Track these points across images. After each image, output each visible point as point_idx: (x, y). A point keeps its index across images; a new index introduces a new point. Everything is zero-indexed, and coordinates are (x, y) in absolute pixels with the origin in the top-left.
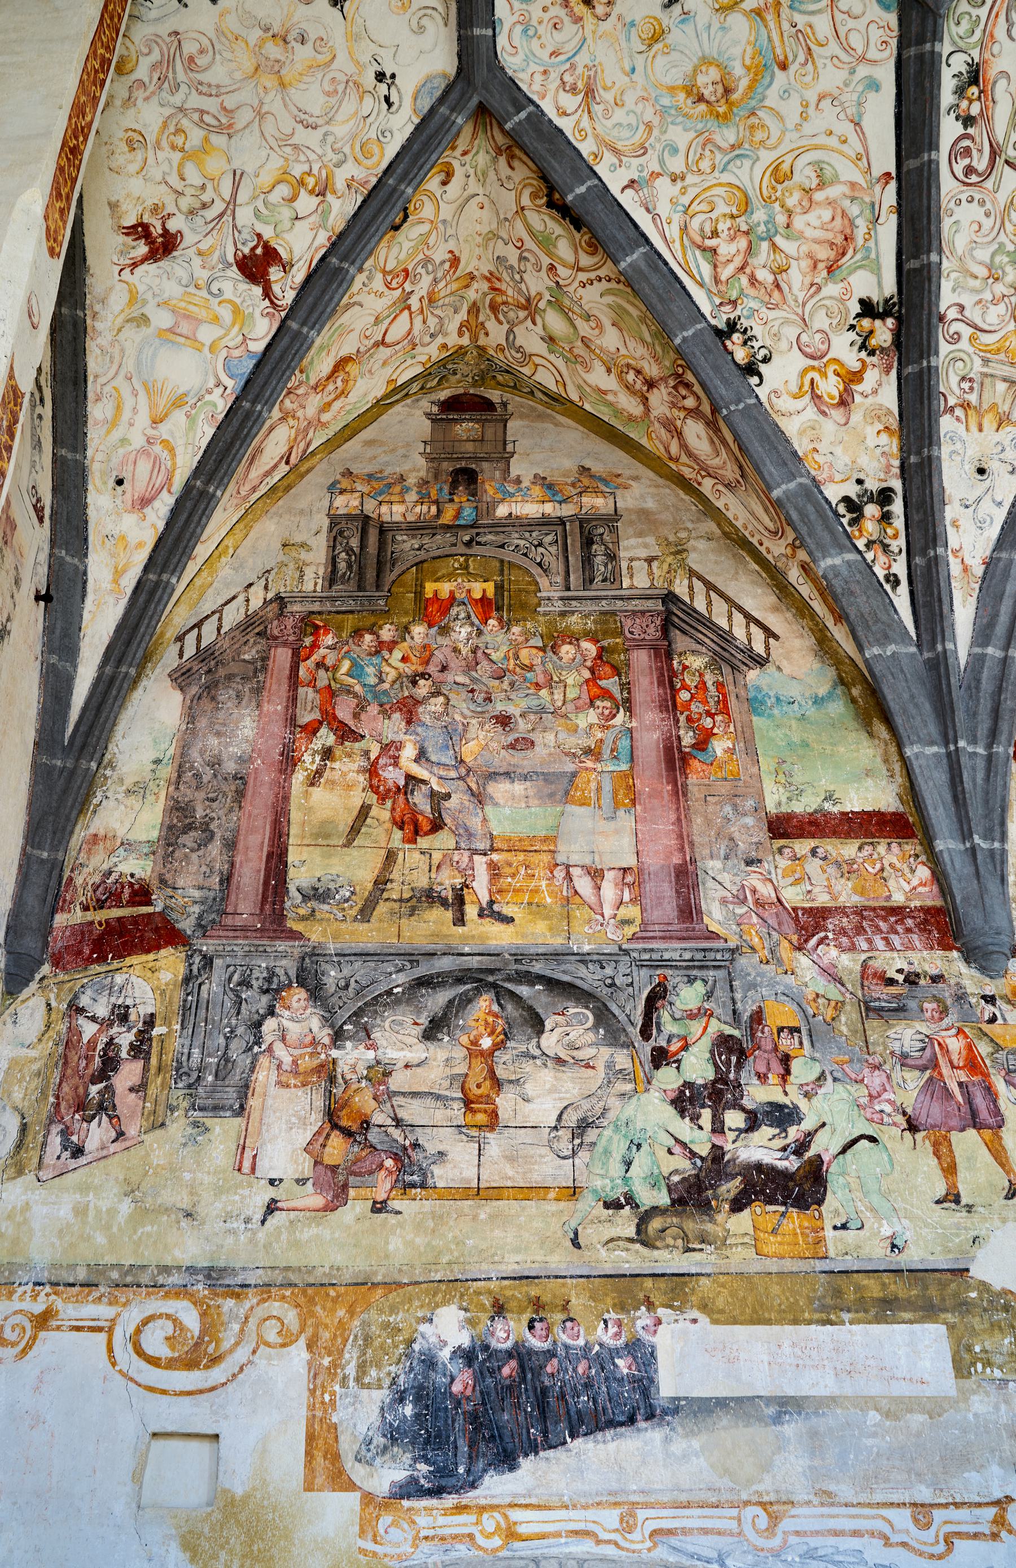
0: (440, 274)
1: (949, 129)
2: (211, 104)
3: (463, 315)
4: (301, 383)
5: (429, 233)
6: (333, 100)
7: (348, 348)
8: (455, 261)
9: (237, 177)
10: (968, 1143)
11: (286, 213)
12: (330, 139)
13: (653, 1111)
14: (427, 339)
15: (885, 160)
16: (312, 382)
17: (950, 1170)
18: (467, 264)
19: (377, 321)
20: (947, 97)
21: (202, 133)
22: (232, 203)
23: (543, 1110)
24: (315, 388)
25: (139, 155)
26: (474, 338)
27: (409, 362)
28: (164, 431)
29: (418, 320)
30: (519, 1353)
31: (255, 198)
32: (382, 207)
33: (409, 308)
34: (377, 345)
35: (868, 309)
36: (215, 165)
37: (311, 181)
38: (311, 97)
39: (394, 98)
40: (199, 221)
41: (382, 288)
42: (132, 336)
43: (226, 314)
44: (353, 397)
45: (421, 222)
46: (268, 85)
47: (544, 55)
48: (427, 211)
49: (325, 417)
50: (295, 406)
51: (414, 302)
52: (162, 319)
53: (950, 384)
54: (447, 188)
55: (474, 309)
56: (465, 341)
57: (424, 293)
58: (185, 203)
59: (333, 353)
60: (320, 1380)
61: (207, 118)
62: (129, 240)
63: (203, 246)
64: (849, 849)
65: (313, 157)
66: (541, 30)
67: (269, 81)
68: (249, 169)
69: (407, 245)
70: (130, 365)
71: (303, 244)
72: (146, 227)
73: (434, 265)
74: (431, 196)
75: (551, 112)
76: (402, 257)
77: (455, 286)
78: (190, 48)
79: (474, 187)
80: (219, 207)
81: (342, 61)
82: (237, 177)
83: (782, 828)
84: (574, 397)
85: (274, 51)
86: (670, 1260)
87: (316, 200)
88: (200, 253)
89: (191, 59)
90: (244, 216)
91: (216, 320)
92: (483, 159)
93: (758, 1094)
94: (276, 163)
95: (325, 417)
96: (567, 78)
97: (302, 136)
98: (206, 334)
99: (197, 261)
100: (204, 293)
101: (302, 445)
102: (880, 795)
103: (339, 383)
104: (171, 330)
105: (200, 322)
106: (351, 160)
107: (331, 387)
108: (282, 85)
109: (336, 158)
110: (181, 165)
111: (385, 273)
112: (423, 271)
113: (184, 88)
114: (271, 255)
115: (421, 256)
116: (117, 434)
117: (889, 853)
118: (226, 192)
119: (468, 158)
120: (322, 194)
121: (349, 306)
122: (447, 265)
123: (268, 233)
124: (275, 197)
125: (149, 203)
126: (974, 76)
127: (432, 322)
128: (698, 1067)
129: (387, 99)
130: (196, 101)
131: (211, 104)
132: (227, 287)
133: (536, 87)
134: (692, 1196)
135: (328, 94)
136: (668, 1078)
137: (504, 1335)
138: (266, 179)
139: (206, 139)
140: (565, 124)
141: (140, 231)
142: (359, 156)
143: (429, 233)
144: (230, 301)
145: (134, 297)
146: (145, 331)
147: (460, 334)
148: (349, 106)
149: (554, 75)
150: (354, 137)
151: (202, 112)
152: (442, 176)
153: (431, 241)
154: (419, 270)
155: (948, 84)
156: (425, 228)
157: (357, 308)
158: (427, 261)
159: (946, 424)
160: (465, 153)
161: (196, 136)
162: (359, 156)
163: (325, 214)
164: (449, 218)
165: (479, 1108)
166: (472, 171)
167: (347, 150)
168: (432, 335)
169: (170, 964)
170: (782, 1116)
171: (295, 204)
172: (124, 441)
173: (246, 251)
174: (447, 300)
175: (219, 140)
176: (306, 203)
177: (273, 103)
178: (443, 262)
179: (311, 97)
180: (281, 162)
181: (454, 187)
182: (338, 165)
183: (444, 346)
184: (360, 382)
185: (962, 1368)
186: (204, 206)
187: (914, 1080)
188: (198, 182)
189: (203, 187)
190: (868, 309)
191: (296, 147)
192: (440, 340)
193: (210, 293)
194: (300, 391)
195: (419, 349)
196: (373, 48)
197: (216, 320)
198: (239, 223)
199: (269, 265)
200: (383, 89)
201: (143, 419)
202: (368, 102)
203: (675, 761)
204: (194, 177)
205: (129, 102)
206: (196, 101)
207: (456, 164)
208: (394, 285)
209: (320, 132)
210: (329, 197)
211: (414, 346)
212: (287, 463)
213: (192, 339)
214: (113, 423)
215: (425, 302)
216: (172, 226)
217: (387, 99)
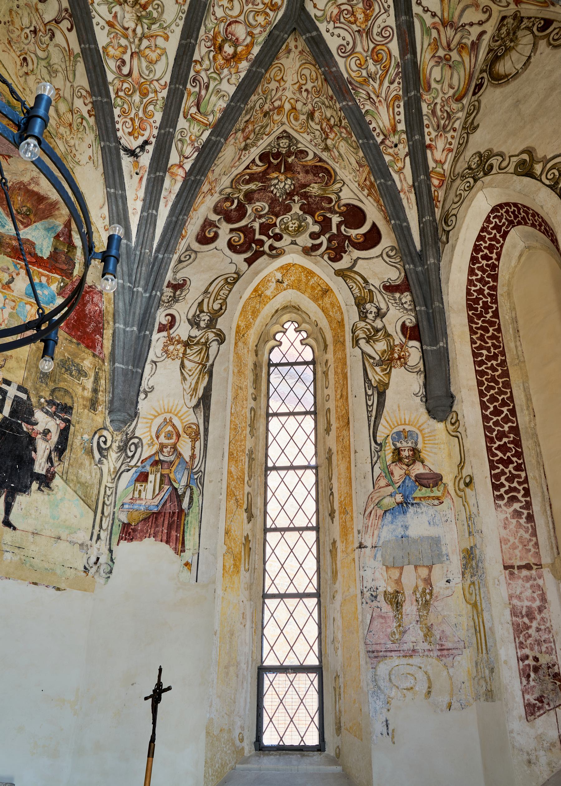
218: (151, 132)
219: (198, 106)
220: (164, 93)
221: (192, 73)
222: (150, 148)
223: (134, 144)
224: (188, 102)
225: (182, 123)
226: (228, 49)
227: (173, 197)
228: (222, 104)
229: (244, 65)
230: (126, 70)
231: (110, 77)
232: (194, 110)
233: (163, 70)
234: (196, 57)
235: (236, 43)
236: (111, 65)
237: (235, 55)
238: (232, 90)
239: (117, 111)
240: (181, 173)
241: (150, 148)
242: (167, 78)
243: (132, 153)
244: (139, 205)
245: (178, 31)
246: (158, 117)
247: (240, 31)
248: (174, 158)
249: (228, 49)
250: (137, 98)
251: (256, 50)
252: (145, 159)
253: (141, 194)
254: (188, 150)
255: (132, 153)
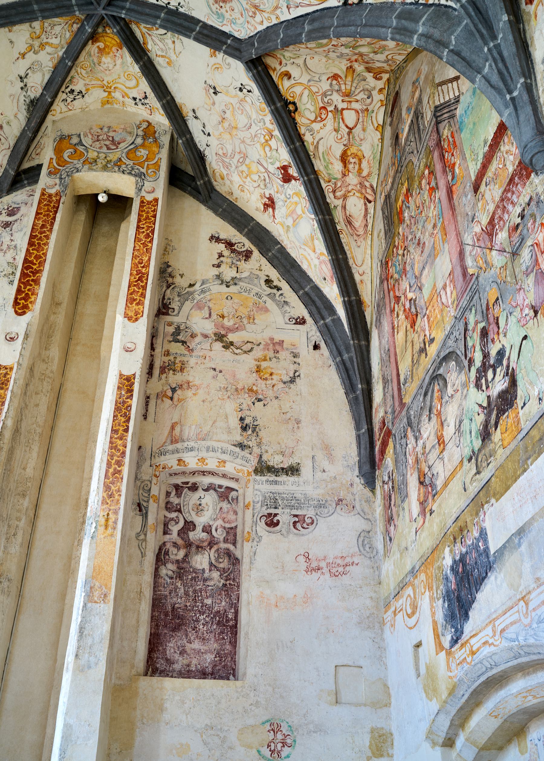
0: (337, 87)
2: (237, 157)
3: (369, 76)
4: (335, 184)
5: (310, 91)
6: (244, 113)
7: (338, 150)
8: (335, 77)
9: (259, 163)
11: (274, 153)
12: (256, 121)
14: (369, 101)
16: (339, 176)
18: (341, 69)
19: (337, 130)
21: (244, 165)
22: (266, 170)
24: (344, 175)
25: (245, 190)
26: (386, 72)
27: (374, 115)
28: (317, 251)
29: (355, 105)
31: (267, 161)
32: (284, 113)
33: (343, 109)
34: (349, 134)
36: (254, 167)
37: (267, 137)
38: (242, 120)
39: (249, 88)
40: (268, 185)
41: (321, 124)
42: (291, 235)
43: (296, 199)
44: (367, 153)
45: (301, 95)
46: (235, 133)
47: (242, 20)
48: (298, 90)
49: (365, 173)
50: (344, 189)
51: (341, 106)
52: (290, 222)
54: (292, 77)
55: (369, 70)
56: (385, 76)
57: (340, 99)
58: (262, 186)
59: (333, 160)
61: (241, 161)
62: (267, 212)
63: (276, 190)
65: (259, 132)
66: (234, 17)
67: (234, 132)
68: (258, 157)
69: (309, 106)
70: (298, 244)
71: (284, 156)
72: (265, 204)
73: (328, 90)
74: (292, 86)
75: (260, 28)
76: (312, 108)
77: (349, 79)
78: (221, 152)
79: (300, 61)
80: (266, 175)
81: (234, 101)
82: (259, 163)
84: (406, 52)
85: (226, 124)
87: (273, 139)
88: (277, 192)
89: (224, 154)
90: (271, 169)
91: (296, 203)
92: (287, 54)
94: (258, 146)
95: (365, 173)
96: (251, 14)
97: (253, 130)
98: (299, 212)
99: (279, 195)
100: (288, 201)
101: (369, 191)
103: (352, 161)
104: (294, 221)
105: (295, 210)
106: (264, 117)
107: (351, 166)
108: (236, 128)
109: (262, 123)
110: (251, 179)
111: (314, 121)
112: (328, 97)
113: (231, 162)
114: (285, 168)
115: (319, 98)
116: (313, 267)
118: (263, 170)
119: (284, 61)
120: (272, 136)
121: (317, 147)
122: (334, 82)
123: (278, 165)
124: (269, 154)
125: (259, 198)
127: (362, 96)
129: (249, 91)
130: (235, 160)
131: (237, 157)
132: (289, 192)
133: (252, 29)
135: (242, 113)
138: (262, 153)
139: (246, 165)
140: (266, 24)
141: (266, 206)
142: (264, 113)
143: (310, 91)
144: (293, 194)
145: (282, 225)
146: (291, 229)
147: (380, 79)
148: (248, 108)
149: (250, 19)
150: (257, 112)
151: (238, 161)
152: (285, 78)
153: (314, 89)
154: (326, 100)
156: (306, 92)
157: (321, 142)
158: (325, 95)
160: (281, 63)
161: (244, 168)
162: (264, 113)
163: (278, 139)
164: (309, 77)
166: (292, 60)
167: (261, 117)
168: (368, 98)
171: (273, 148)
172: (315, 266)
173: (281, 176)
174: (355, 85)
175: (247, 161)
176: (273, 143)
177: (241, 135)
178: (331, 85)
179: (242, 120)
180: (258, 144)
181: (295, 72)
182: (265, 124)
183: (381, 90)
184: (363, 148)
186: (265, 180)
188: (258, 177)
189: (259, 176)
191: (255, 136)
192: (375, 93)
193: (289, 199)
194: (339, 184)
195: (370, 108)
196: (232, 87)
197: (296, 203)
198: (273, 172)
199: (287, 171)
200: (245, 91)
201: (312, 254)
202: (247, 99)
204: (255, 177)
205: (231, 182)
206: (235, 160)
207: (284, 69)
208: (323, 116)
209: (253, 123)
210: (274, 133)
211: (367, 110)
212: (370, 202)
213: (299, 216)
214: (310, 265)
215: (347, 99)
216: (268, 196)
217: (249, 91)
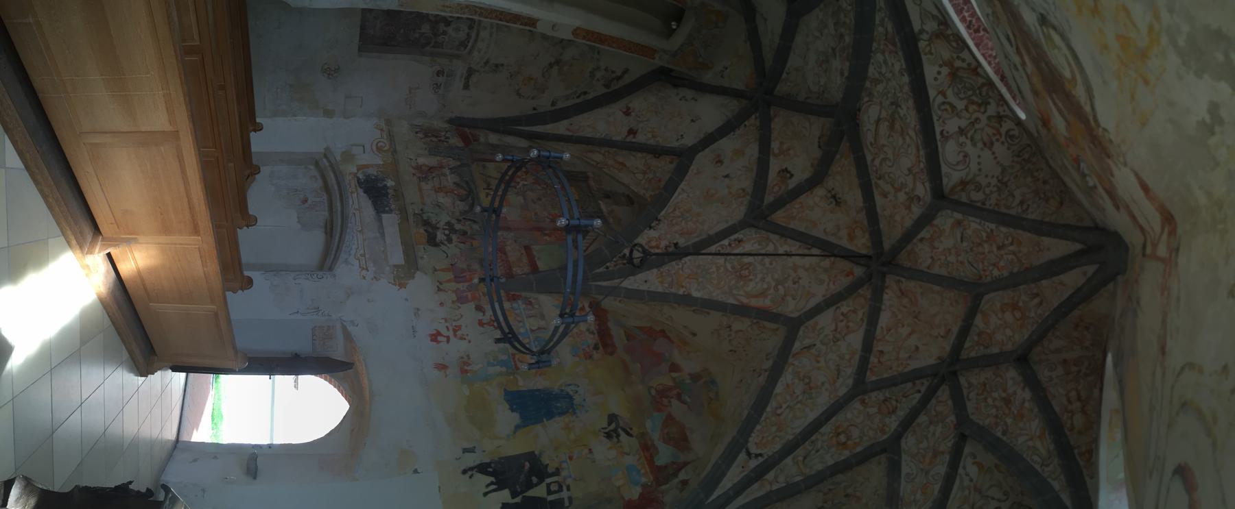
1: (726, 242)
10: (450, 276)
13: (445, 218)
15: (712, 232)
17: (443, 270)
20: (733, 237)
23: (441, 200)
30: (387, 194)
35: (676, 245)
53: (665, 268)
60: (378, 166)
64: (525, 260)
83: (527, 249)
86: (411, 219)
93: (454, 237)
102: (542, 266)
117: (527, 269)
126: (740, 241)
128: (458, 227)
134: (427, 223)
136: (454, 221)
137: (390, 191)
155: (736, 236)
159: (655, 271)
165: (439, 190)
169: (461, 144)
170: (450, 240)
185: (395, 266)
187: (464, 266)
190: (676, 245)
203: (539, 229)
218: (768, 451)
219: (805, 458)
220: (791, 437)
221: (813, 438)
222: (761, 460)
223: (754, 450)
224: (800, 452)
225: (789, 460)
226: (842, 438)
227: (753, 497)
228: (820, 467)
229: (847, 453)
230: (779, 412)
231: (768, 409)
232: (801, 458)
233: (800, 425)
234: (822, 430)
235: (849, 438)
236: (773, 404)
237: (844, 444)
238: (830, 462)
239: (758, 427)
240: (768, 488)
241: (761, 460)
242: (798, 431)
243: (749, 454)
244: (729, 485)
245: (820, 411)
246: (778, 447)
247: (855, 433)
248: (770, 476)
249: (842, 438)
250: (774, 429)
251: (859, 449)
252: (754, 463)
253: (736, 480)
254: (781, 479)
255: (749, 454)
